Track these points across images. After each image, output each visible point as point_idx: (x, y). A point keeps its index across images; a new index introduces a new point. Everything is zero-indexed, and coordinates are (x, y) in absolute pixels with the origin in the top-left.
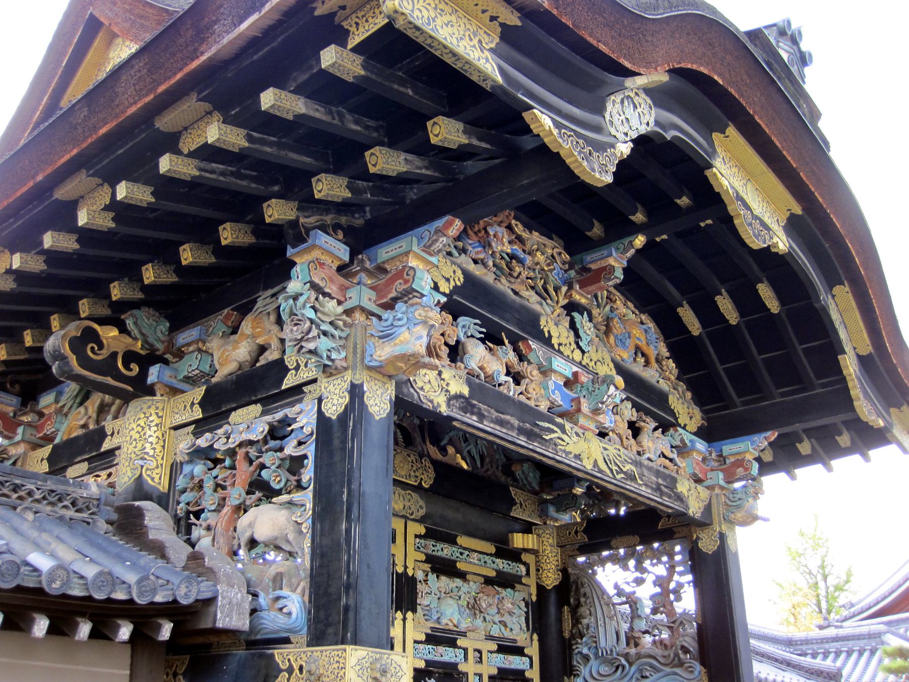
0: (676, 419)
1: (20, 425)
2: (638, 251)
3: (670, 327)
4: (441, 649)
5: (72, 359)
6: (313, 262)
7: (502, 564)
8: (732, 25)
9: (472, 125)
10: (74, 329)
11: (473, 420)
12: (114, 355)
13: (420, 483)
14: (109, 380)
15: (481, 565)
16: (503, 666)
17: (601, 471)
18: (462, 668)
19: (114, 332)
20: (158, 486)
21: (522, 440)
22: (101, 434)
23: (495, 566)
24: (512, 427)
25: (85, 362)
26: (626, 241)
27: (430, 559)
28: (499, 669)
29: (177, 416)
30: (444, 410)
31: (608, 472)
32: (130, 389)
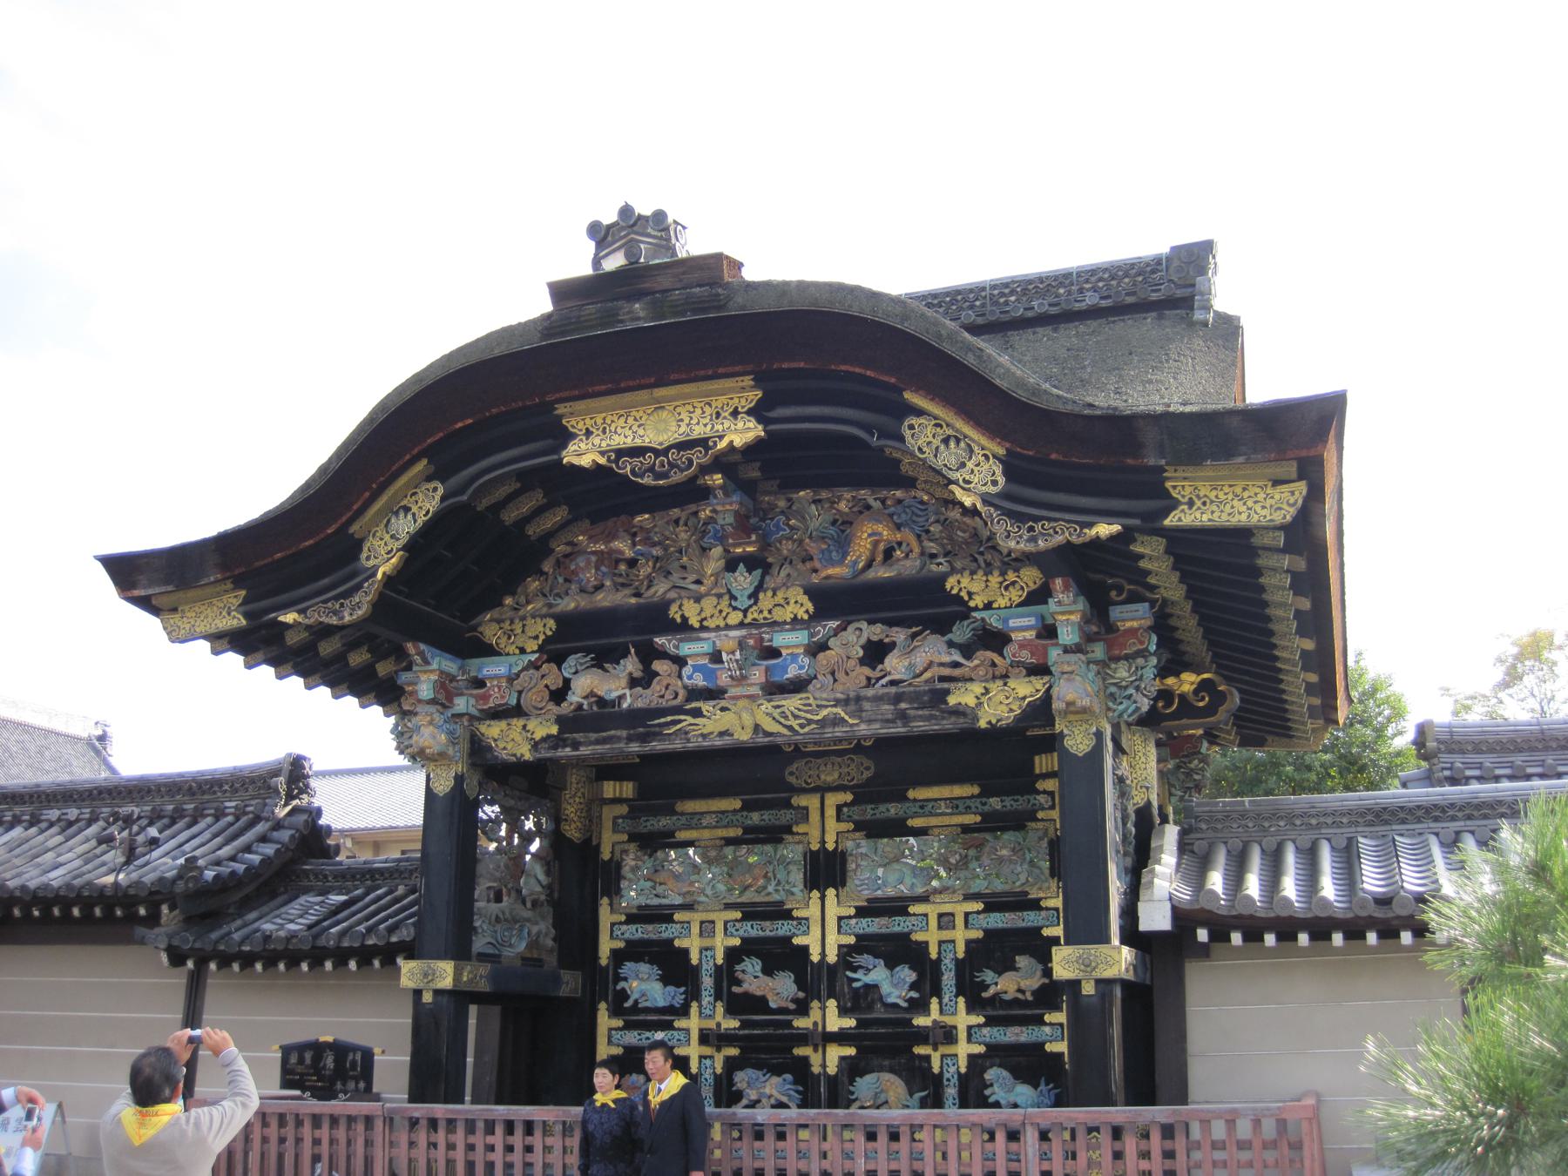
0: (965, 603)
4: (884, 921)
7: (995, 803)
11: (568, 751)
15: (961, 813)
16: (1000, 925)
17: (771, 734)
18: (918, 937)
21: (635, 747)
23: (986, 808)
24: (619, 739)
27: (859, 826)
28: (986, 931)
30: (528, 756)
31: (785, 731)
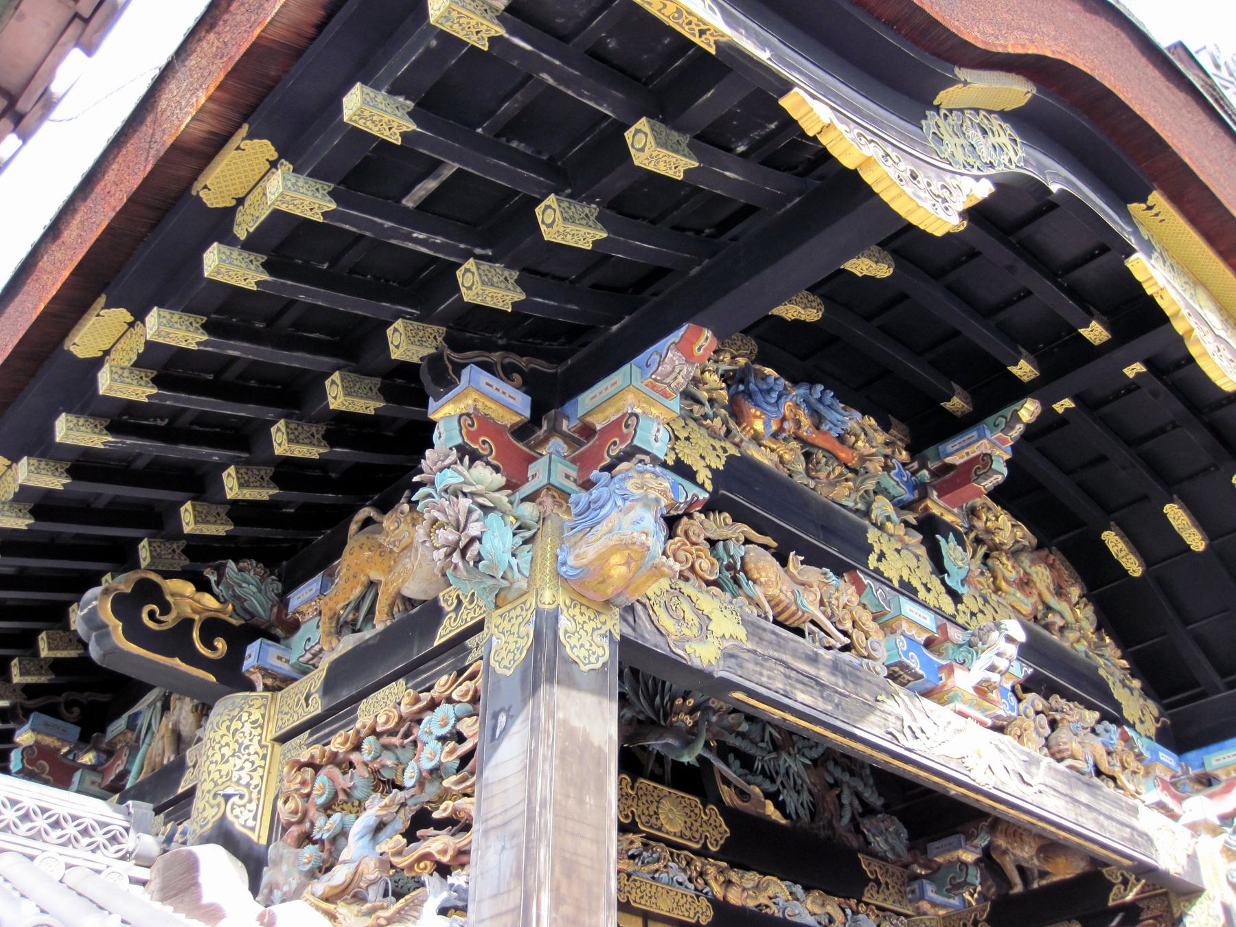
1: (77, 769)
2: (1028, 426)
3: (1095, 573)
5: (116, 627)
6: (468, 415)
8: (1131, 14)
9: (709, 140)
10: (124, 583)
12: (186, 624)
13: (705, 846)
14: (176, 662)
19: (189, 588)
20: (250, 834)
22: (179, 767)
25: (135, 632)
26: (1008, 412)
29: (286, 717)
32: (212, 678)
